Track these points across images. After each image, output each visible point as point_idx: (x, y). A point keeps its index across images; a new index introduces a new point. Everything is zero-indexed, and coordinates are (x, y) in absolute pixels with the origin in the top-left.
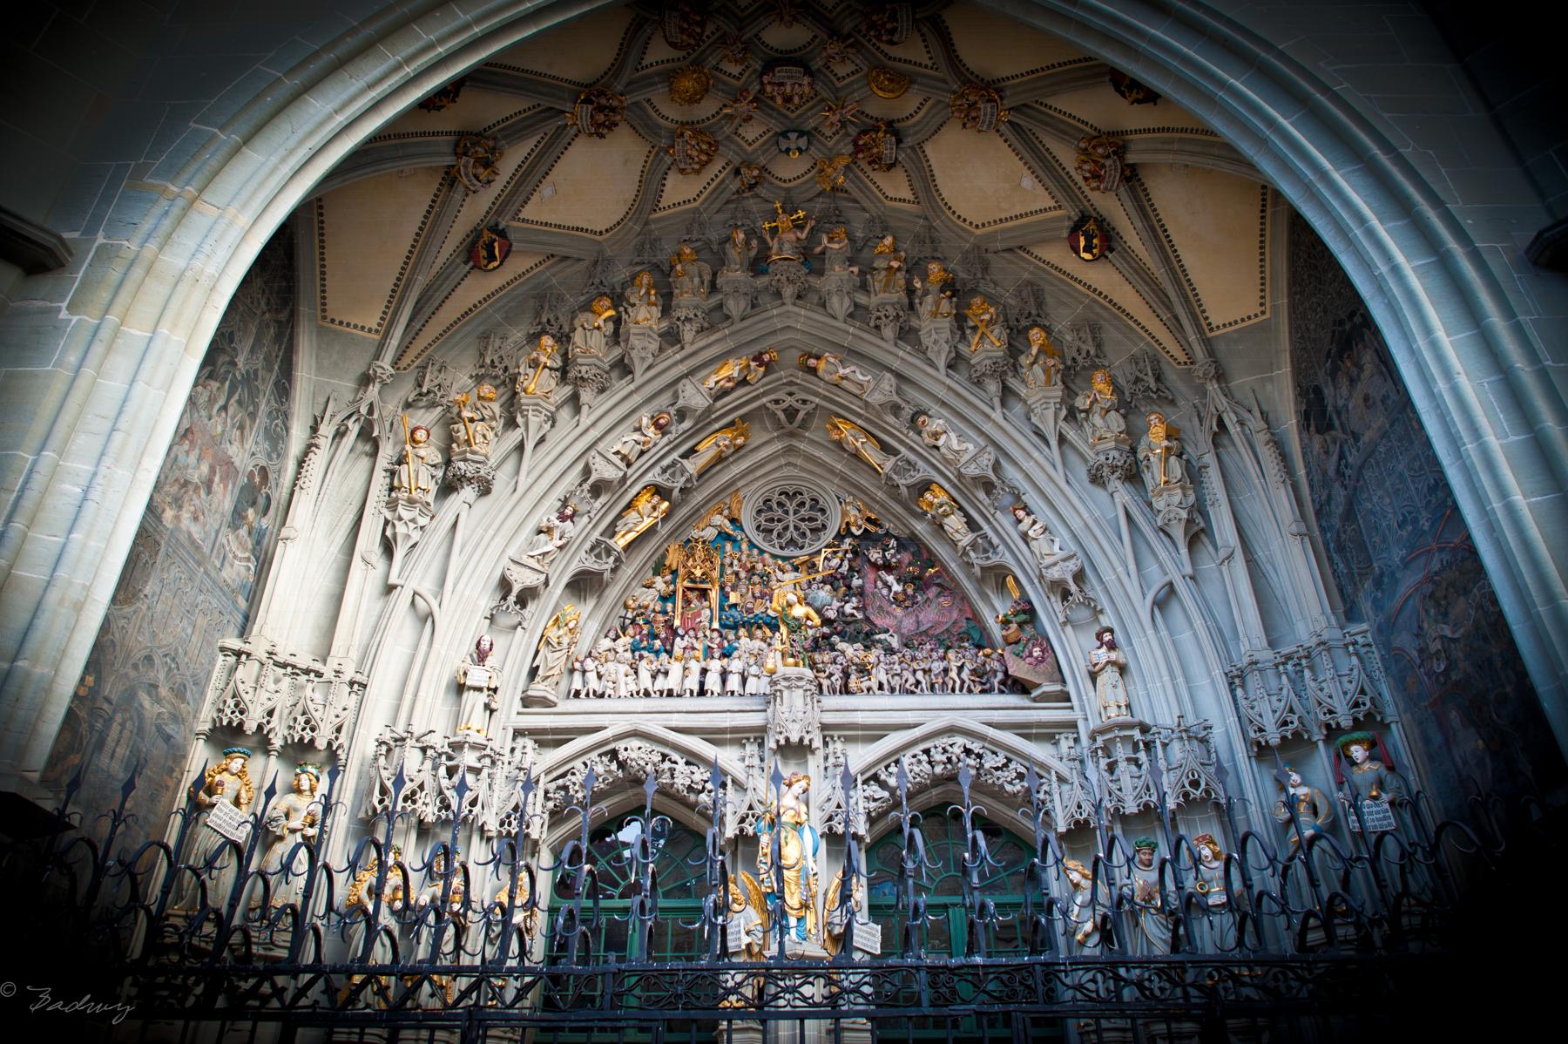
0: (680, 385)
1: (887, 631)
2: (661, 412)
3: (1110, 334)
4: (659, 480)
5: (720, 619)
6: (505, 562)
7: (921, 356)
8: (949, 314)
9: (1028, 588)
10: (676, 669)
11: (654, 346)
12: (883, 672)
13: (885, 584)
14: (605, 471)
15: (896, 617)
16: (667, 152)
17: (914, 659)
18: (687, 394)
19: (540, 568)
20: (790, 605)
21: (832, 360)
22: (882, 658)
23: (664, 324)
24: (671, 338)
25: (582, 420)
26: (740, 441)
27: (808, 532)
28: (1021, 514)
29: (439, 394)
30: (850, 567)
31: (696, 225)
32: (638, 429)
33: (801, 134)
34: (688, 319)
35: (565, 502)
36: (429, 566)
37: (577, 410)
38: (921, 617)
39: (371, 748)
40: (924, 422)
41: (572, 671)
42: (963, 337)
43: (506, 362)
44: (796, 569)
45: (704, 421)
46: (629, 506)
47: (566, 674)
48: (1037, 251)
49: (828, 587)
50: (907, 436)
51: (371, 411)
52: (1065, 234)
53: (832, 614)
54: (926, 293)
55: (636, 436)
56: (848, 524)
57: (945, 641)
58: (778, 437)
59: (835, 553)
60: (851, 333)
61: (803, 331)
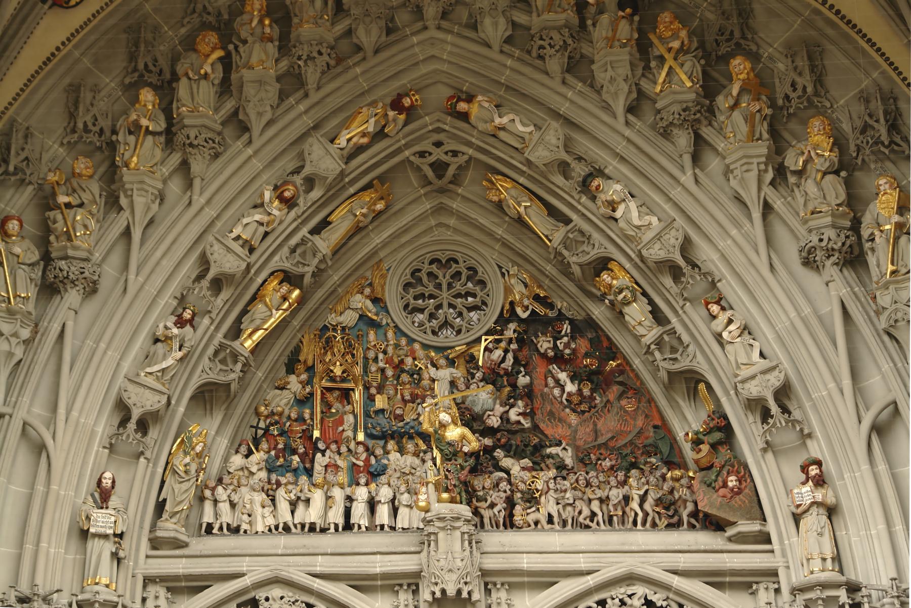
0: (306, 147)
4: (287, 265)
6: (120, 381)
11: (273, 90)
13: (557, 381)
18: (314, 156)
23: (284, 64)
25: (195, 197)
28: (715, 308)
29: (28, 174)
30: (516, 358)
34: (310, 58)
35: (182, 300)
37: (189, 185)
41: (202, 499)
46: (254, 298)
47: (196, 503)
49: (490, 387)
53: (494, 422)
56: (512, 304)
59: (498, 341)
61: (450, 62)
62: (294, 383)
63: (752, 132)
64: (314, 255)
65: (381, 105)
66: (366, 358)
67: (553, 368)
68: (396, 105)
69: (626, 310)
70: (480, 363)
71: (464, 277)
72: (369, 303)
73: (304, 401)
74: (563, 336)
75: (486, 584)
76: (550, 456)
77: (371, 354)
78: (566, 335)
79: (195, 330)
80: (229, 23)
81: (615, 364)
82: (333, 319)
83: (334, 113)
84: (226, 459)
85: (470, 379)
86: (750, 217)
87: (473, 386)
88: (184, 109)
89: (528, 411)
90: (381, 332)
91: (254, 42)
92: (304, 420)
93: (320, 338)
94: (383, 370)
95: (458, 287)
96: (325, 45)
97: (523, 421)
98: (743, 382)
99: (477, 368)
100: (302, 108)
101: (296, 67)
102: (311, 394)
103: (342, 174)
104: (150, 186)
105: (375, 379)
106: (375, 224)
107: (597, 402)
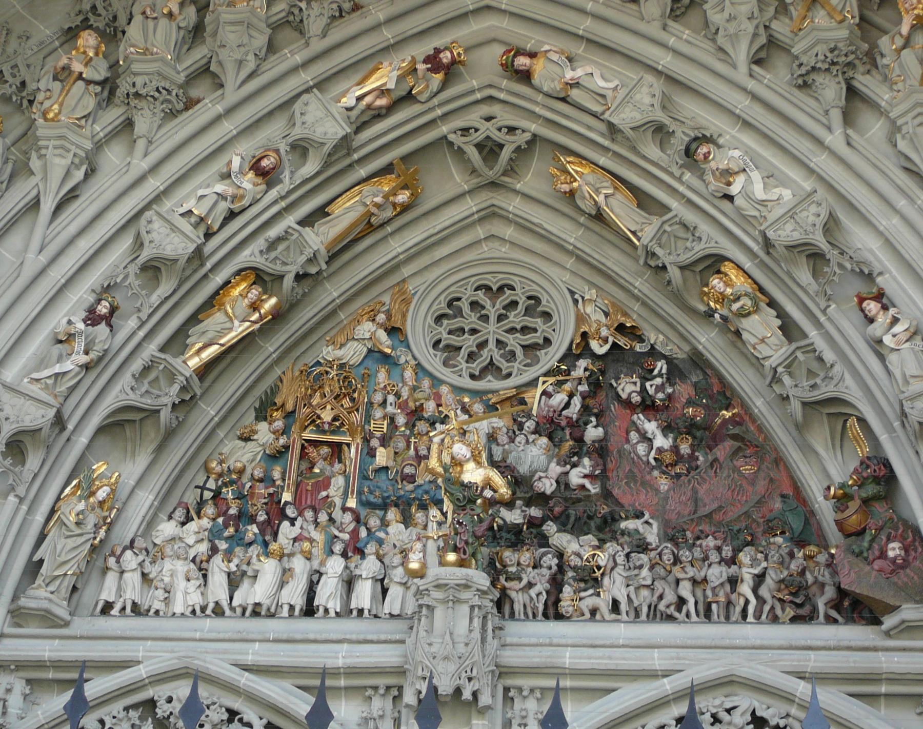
0: (298, 106)
1: (639, 515)
2: (269, 150)
4: (260, 261)
5: (360, 493)
9: (883, 438)
10: (269, 569)
12: (619, 580)
15: (657, 491)
18: (309, 118)
19: (44, 396)
20: (457, 463)
21: (555, 57)
25: (135, 161)
26: (403, 197)
27: (519, 352)
32: (226, 176)
38: (701, 492)
40: (706, 156)
44: (491, 408)
49: (544, 440)
53: (547, 486)
55: (220, 188)
56: (584, 335)
67: (639, 418)
70: (534, 412)
74: (655, 377)
78: (660, 375)
81: (730, 414)
85: (516, 430)
87: (520, 439)
88: (132, 49)
89: (597, 472)
97: (588, 485)
98: (912, 399)
99: (529, 416)
101: (296, 11)
104: (73, 143)
107: (699, 463)
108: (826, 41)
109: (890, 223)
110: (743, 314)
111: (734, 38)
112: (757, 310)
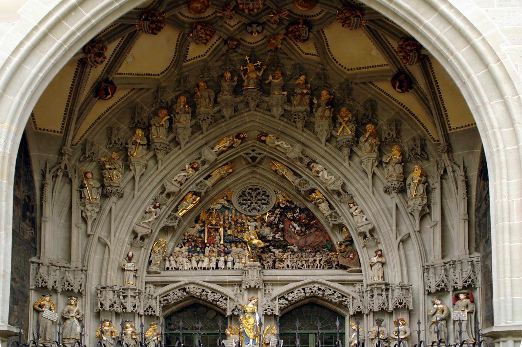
0: (202, 150)
3: (405, 126)
4: (195, 189)
7: (314, 136)
8: (329, 117)
11: (189, 130)
14: (172, 188)
16: (189, 35)
17: (302, 256)
18: (205, 154)
21: (273, 138)
22: (289, 257)
23: (194, 122)
24: (196, 128)
31: (206, 69)
33: (259, 24)
36: (103, 227)
38: (307, 239)
39: (94, 290)
40: (313, 166)
42: (335, 127)
43: (121, 141)
45: (214, 165)
46: (182, 200)
48: (377, 84)
50: (305, 171)
51: (66, 166)
52: (390, 79)
54: (319, 107)
57: (316, 249)
58: (248, 167)
60: (282, 125)
62: (198, 226)
63: (372, 148)
64: (205, 186)
65: (231, 137)
66: (224, 219)
68: (238, 137)
69: (320, 205)
71: (261, 194)
72: (226, 202)
73: (202, 232)
75: (265, 284)
76: (289, 248)
77: (226, 218)
79: (160, 210)
80: (171, 107)
82: (212, 207)
83: (213, 139)
84: (173, 249)
86: (367, 177)
90: (230, 211)
91: (182, 114)
92: (201, 238)
93: (207, 212)
94: (230, 223)
95: (259, 197)
96: (210, 115)
100: (200, 137)
101: (198, 123)
102: (204, 230)
103: (216, 160)
105: (228, 226)
106: (228, 177)
108: (346, 139)
109: (357, 185)
110: (320, 203)
111: (322, 136)
112: (323, 202)
